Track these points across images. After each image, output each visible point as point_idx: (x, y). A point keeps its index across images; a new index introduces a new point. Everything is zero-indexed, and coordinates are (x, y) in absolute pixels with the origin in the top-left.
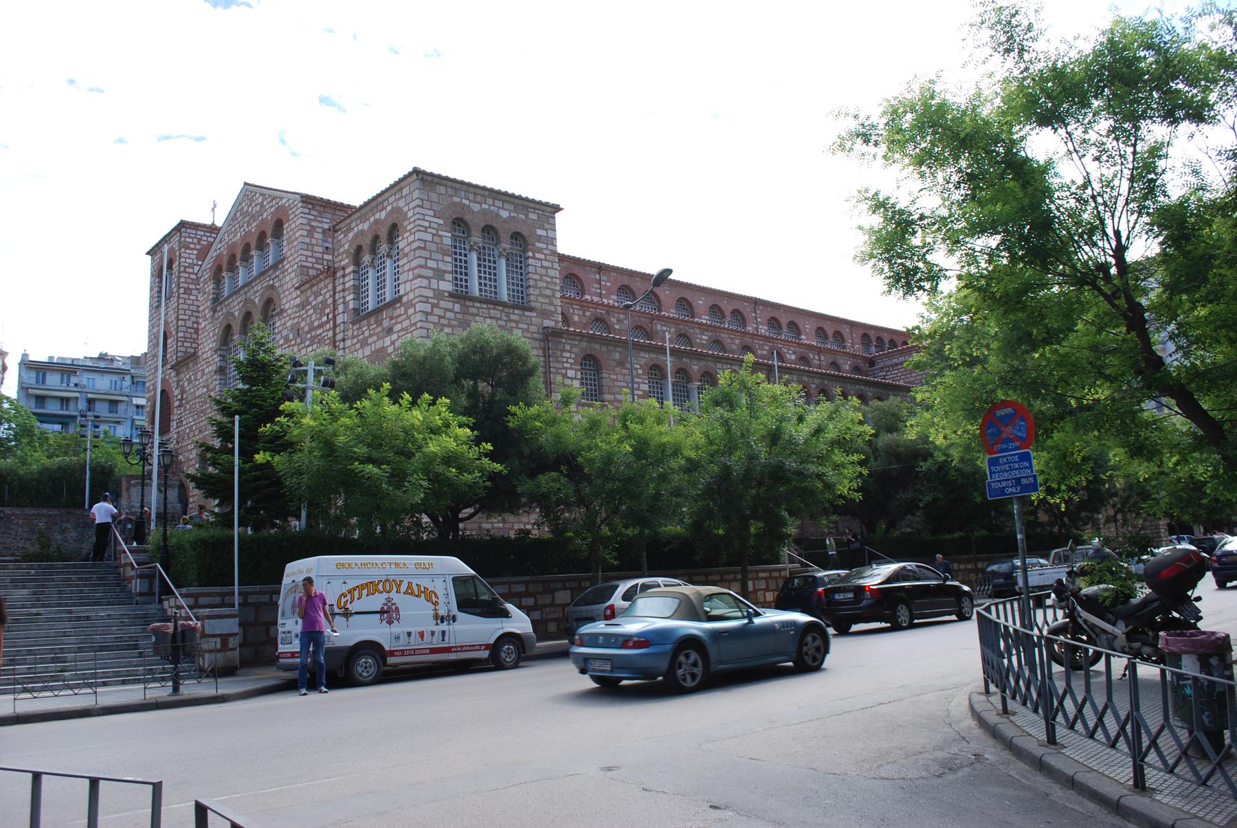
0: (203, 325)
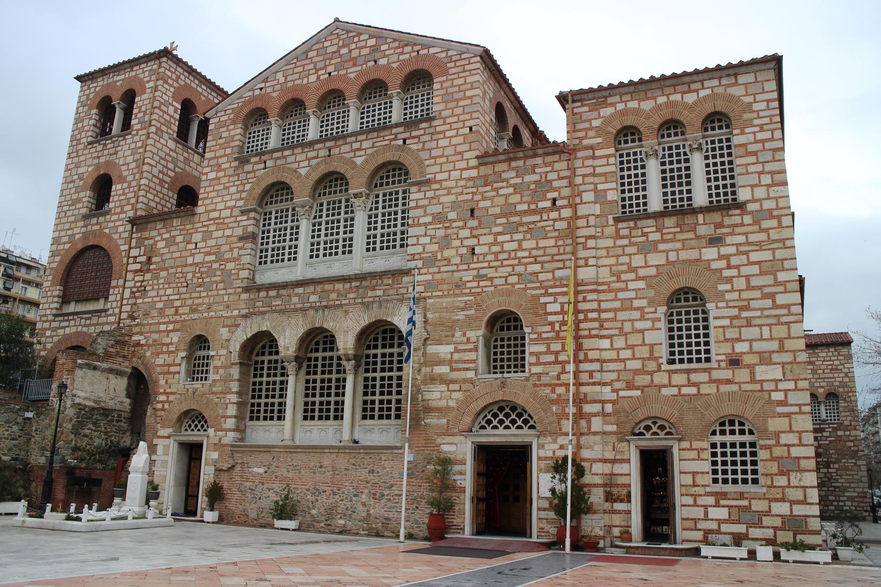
0: (212, 175)
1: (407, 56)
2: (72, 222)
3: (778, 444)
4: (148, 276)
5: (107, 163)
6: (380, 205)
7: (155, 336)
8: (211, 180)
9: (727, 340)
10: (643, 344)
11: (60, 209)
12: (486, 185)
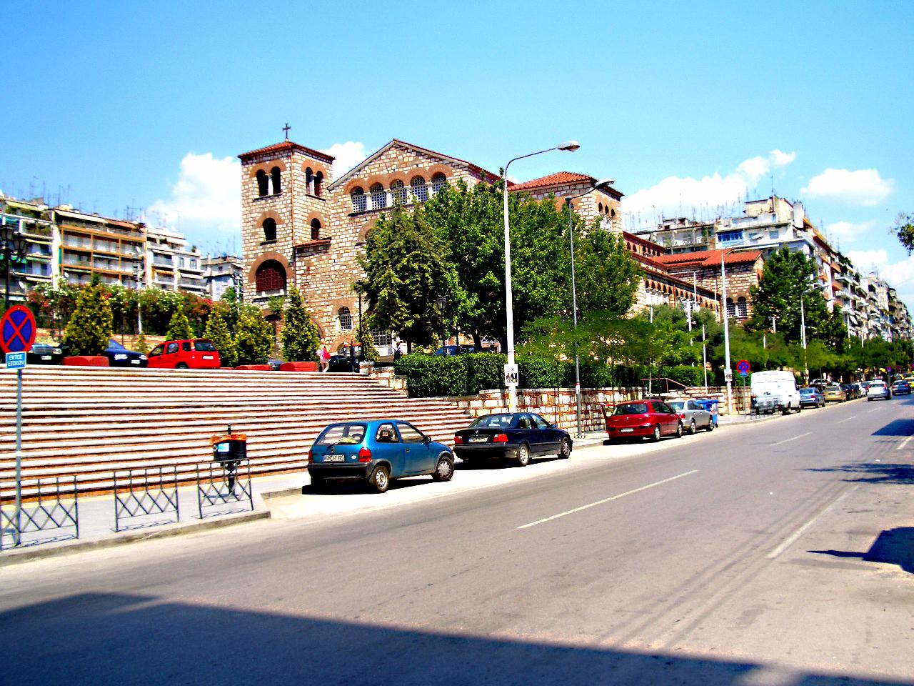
0: (337, 223)
2: (254, 246)
4: (309, 277)
5: (270, 212)
7: (320, 308)
11: (244, 238)
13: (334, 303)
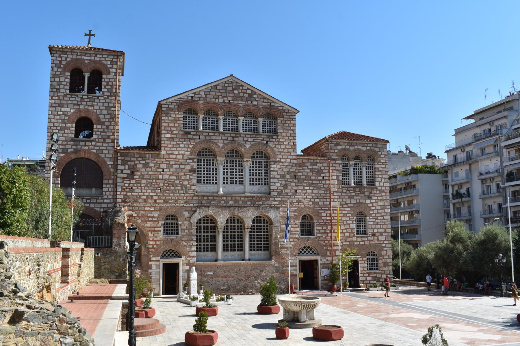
0: (168, 136)
1: (266, 104)
3: (384, 259)
4: (133, 181)
6: (255, 166)
8: (168, 138)
9: (372, 228)
10: (350, 228)
12: (300, 167)
13: (160, 209)
